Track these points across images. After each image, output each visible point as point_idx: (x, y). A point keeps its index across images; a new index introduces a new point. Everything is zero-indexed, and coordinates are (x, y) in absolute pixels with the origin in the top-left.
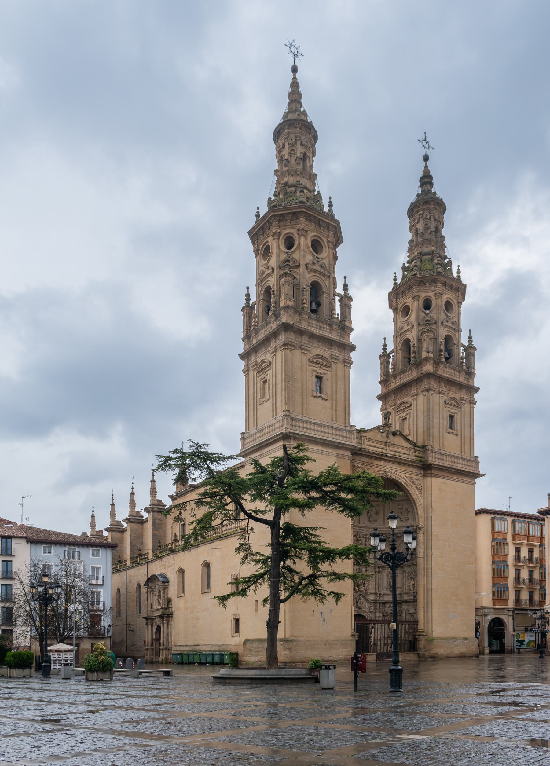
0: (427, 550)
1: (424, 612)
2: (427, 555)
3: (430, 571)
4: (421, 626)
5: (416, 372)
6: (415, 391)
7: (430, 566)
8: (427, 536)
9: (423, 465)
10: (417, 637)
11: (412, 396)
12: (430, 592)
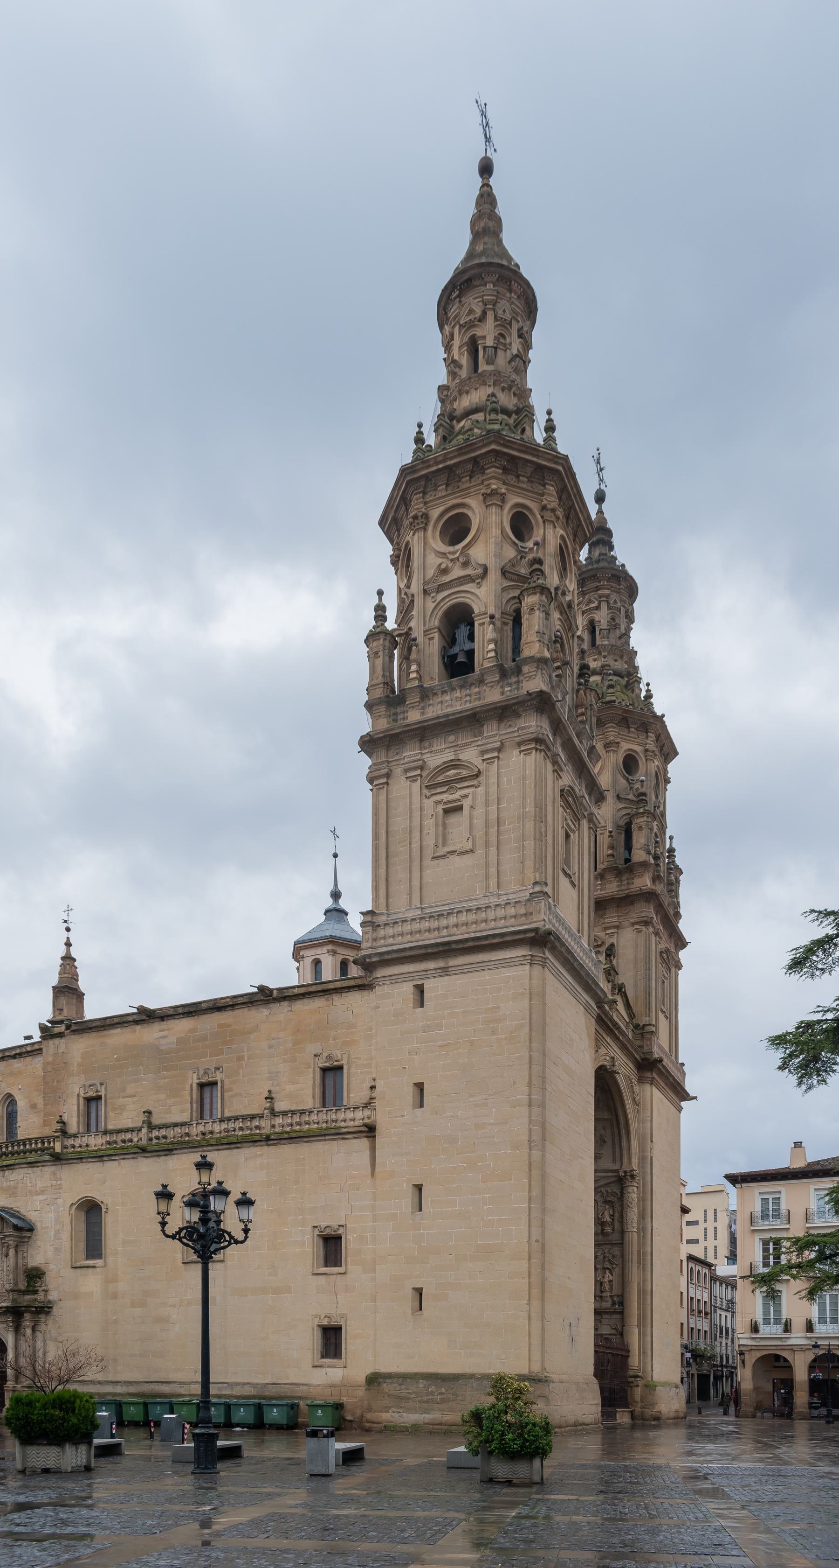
0: (643, 1218)
1: (639, 1334)
2: (644, 1229)
4: (634, 1361)
6: (615, 919)
8: (644, 1192)
9: (643, 1059)
10: (630, 1380)
11: (606, 929)
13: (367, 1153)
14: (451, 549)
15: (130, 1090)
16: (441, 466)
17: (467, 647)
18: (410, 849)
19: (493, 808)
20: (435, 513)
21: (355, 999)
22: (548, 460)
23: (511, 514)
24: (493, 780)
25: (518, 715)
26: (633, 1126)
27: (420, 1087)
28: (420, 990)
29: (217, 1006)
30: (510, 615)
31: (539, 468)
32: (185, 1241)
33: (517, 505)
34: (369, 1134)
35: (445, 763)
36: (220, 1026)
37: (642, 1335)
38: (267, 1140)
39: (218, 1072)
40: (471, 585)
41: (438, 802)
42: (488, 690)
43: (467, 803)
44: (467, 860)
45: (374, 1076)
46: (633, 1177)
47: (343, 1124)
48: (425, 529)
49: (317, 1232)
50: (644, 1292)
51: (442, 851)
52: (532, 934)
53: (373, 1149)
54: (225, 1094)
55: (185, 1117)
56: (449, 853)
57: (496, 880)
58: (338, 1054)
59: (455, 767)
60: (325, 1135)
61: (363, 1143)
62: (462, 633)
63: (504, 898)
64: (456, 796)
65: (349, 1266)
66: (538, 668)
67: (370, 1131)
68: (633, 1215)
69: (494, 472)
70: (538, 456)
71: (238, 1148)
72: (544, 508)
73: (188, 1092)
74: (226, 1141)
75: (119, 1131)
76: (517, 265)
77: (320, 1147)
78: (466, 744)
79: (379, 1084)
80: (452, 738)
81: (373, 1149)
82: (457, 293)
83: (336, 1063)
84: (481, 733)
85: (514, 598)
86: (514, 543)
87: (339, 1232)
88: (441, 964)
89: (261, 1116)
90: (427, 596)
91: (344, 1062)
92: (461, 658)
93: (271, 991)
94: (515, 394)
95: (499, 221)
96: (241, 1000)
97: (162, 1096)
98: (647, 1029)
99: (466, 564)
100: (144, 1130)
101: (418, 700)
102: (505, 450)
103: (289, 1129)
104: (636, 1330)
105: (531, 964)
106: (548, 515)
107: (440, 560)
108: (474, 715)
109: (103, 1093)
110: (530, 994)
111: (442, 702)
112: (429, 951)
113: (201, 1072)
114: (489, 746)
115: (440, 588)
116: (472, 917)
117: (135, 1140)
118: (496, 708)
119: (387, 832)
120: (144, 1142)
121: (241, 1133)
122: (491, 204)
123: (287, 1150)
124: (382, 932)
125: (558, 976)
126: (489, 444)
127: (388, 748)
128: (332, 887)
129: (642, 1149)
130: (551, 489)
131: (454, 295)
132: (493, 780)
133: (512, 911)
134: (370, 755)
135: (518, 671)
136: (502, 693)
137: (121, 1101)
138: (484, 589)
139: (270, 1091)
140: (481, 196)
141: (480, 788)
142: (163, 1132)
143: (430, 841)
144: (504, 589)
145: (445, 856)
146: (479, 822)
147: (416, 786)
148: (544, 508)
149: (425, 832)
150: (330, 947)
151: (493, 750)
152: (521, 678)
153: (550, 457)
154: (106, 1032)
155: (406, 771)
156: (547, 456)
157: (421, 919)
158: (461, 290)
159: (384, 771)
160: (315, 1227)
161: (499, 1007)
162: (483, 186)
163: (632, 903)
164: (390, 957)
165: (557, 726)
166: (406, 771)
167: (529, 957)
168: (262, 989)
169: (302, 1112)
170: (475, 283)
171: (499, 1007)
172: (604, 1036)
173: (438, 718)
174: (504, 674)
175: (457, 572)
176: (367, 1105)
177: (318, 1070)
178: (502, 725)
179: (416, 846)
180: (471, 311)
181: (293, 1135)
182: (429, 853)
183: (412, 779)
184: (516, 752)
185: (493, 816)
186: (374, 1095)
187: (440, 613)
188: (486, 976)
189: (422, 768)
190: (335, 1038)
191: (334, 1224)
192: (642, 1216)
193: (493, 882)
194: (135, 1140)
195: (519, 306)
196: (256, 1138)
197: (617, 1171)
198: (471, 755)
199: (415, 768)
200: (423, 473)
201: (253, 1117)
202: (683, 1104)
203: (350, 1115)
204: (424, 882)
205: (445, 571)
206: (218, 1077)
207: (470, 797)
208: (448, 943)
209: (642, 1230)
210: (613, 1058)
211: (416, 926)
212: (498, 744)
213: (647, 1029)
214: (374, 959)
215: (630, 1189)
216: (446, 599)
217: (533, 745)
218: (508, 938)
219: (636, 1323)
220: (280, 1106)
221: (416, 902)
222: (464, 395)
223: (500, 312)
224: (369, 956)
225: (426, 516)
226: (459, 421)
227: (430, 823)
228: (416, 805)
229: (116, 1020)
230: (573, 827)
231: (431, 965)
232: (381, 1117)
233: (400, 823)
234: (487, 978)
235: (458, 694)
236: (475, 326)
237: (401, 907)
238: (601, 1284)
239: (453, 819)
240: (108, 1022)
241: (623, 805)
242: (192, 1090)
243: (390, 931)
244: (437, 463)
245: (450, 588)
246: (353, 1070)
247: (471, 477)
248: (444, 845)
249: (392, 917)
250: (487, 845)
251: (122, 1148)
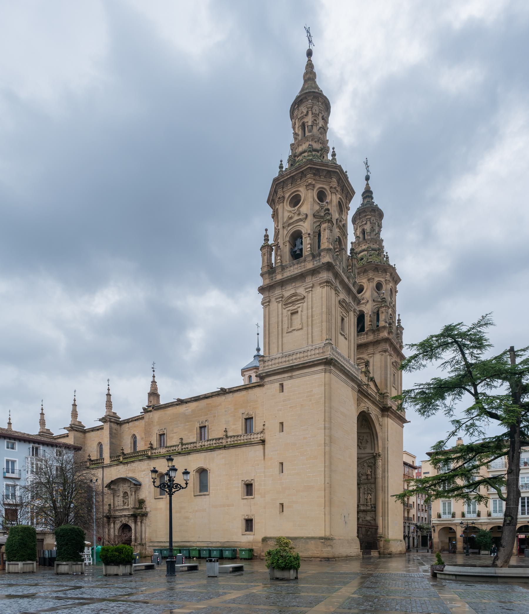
0: (384, 472)
1: (382, 520)
2: (384, 477)
3: (387, 488)
4: (380, 531)
5: (372, 336)
6: (372, 351)
7: (387, 485)
8: (384, 462)
9: (383, 407)
10: (378, 538)
11: (368, 355)
12: (387, 505)
13: (262, 451)
14: (293, 209)
15: (175, 431)
16: (289, 176)
17: (300, 247)
18: (278, 330)
19: (310, 311)
20: (287, 196)
21: (257, 390)
22: (332, 168)
23: (317, 192)
24: (310, 300)
25: (319, 273)
26: (380, 435)
28: (282, 385)
29: (206, 397)
30: (317, 233)
31: (329, 172)
32: (162, 488)
33: (320, 188)
35: (291, 294)
36: (207, 404)
37: (384, 520)
38: (225, 447)
39: (206, 422)
40: (301, 222)
41: (288, 311)
42: (308, 264)
44: (300, 332)
45: (264, 420)
46: (379, 455)
47: (253, 440)
48: (283, 202)
49: (243, 483)
50: (385, 502)
51: (290, 330)
52: (325, 360)
53: (264, 449)
54: (209, 430)
55: (195, 440)
57: (311, 339)
58: (251, 412)
59: (295, 296)
60: (246, 445)
61: (260, 447)
62: (298, 242)
63: (314, 346)
64: (295, 307)
65: (255, 496)
66: (327, 253)
67: (263, 442)
68: (379, 471)
69: (310, 176)
70: (328, 167)
72: (331, 188)
73: (196, 430)
74: (209, 448)
75: (171, 447)
76: (321, 91)
77: (244, 449)
78: (300, 286)
79: (266, 424)
80: (294, 284)
81: (264, 449)
82: (297, 106)
83: (250, 416)
84: (305, 281)
85: (318, 226)
86: (319, 203)
87: (252, 482)
88: (290, 374)
89: (222, 438)
90: (284, 229)
91: (253, 416)
93: (226, 390)
94: (320, 143)
95: (315, 74)
96: (215, 394)
97: (186, 432)
98: (386, 395)
99: (299, 214)
100: (180, 446)
102: (314, 167)
103: (233, 443)
104: (381, 518)
105: (325, 372)
106: (333, 190)
107: (289, 214)
108: (302, 274)
109: (165, 432)
110: (325, 384)
111: (290, 270)
112: (285, 370)
113: (200, 423)
114: (308, 286)
115: (289, 225)
116: (302, 355)
117: (177, 449)
118: (310, 271)
119: (269, 324)
120: (180, 450)
121: (215, 445)
122: (311, 68)
123: (232, 451)
124: (267, 364)
125: (338, 376)
126: (308, 165)
127: (269, 291)
128: (257, 347)
129: (384, 444)
130: (334, 180)
131: (296, 107)
132: (310, 300)
133: (317, 351)
134: (262, 294)
135: (319, 255)
136: (313, 264)
137: (172, 435)
138: (306, 223)
139: (226, 429)
140: (307, 65)
142: (187, 446)
143: (285, 326)
144: (314, 223)
146: (304, 317)
147: (280, 305)
148: (331, 188)
149: (284, 323)
150: (255, 370)
151: (309, 288)
152: (321, 257)
153: (333, 167)
154: (166, 409)
155: (276, 299)
156: (332, 167)
157: (282, 357)
158: (298, 105)
159: (267, 300)
160: (242, 480)
161: (312, 390)
162: (308, 61)
163: (379, 343)
164: (270, 373)
165: (336, 275)
166: (276, 299)
168: (222, 389)
169: (238, 436)
170: (304, 101)
171: (312, 390)
172: (364, 399)
173: (288, 277)
174: (314, 256)
175: (296, 218)
176: (262, 432)
177: (243, 419)
178: (313, 277)
179: (280, 328)
180: (302, 112)
181: (235, 445)
182: (285, 331)
183: (279, 302)
184: (319, 287)
185: (310, 314)
186: (264, 428)
187: (289, 235)
188: (307, 378)
189: (282, 297)
190: (250, 407)
191: (250, 479)
192: (384, 471)
193: (310, 340)
194: (177, 449)
195: (322, 107)
196: (221, 447)
197: (373, 453)
198: (301, 291)
199: (280, 298)
201: (219, 439)
202: (404, 425)
203: (256, 436)
204: (283, 342)
205: (291, 218)
206: (207, 424)
207: (301, 308)
208: (292, 366)
209: (383, 477)
210: (368, 408)
211: (280, 360)
212: (311, 285)
213: (386, 395)
214: (264, 375)
215: (378, 461)
216: (292, 229)
217: (326, 284)
218: (315, 363)
219: (381, 515)
220: (230, 434)
221: (280, 351)
223: (314, 111)
224: (262, 373)
225: (284, 197)
226: (298, 157)
227: (285, 319)
228: (280, 312)
229: (170, 404)
230: (345, 315)
231: (286, 375)
232: (267, 437)
233: (274, 320)
235: (296, 266)
236: (304, 118)
237: (274, 353)
238: (367, 499)
239: (295, 317)
240: (167, 405)
241: (376, 304)
242: (197, 429)
243: (270, 363)
244: (287, 176)
245: (293, 224)
246: (257, 418)
247: (301, 179)
248: (291, 327)
249: (271, 357)
250: (308, 326)
251: (172, 453)
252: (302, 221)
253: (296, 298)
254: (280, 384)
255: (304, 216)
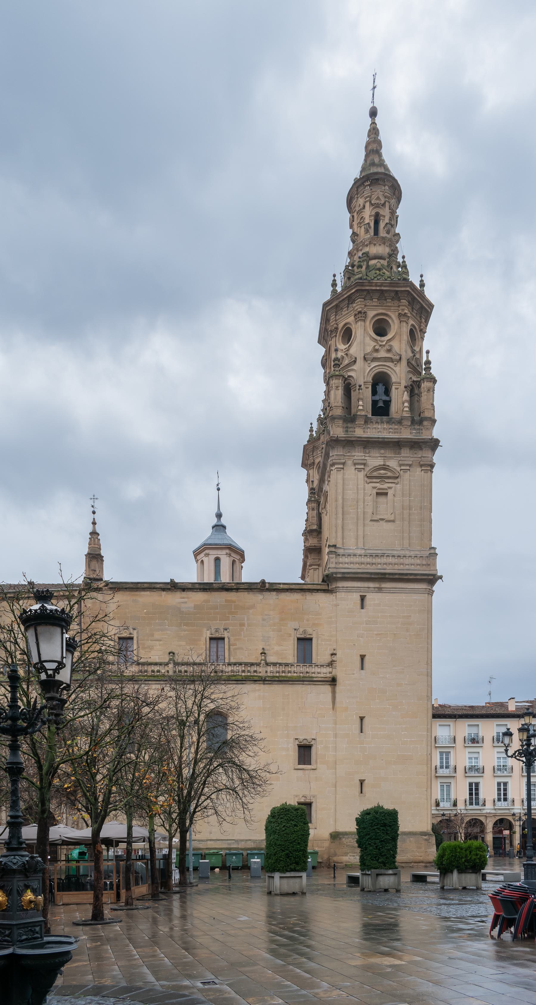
13: (330, 695)
15: (157, 635)
17: (385, 398)
21: (321, 597)
27: (363, 657)
28: (363, 598)
34: (332, 683)
35: (380, 465)
36: (227, 601)
38: (263, 680)
39: (225, 632)
42: (403, 429)
43: (390, 492)
44: (390, 526)
45: (335, 647)
47: (313, 675)
49: (297, 743)
53: (334, 693)
54: (231, 647)
56: (380, 519)
58: (310, 630)
59: (385, 469)
60: (303, 681)
61: (327, 689)
62: (381, 388)
64: (386, 486)
67: (333, 681)
71: (243, 684)
74: (234, 678)
77: (299, 688)
78: (390, 457)
79: (339, 653)
80: (382, 451)
81: (334, 693)
83: (308, 636)
84: (399, 453)
87: (312, 743)
88: (377, 585)
89: (258, 664)
91: (314, 636)
92: (381, 404)
97: (183, 643)
100: (171, 666)
101: (363, 423)
103: (278, 674)
108: (398, 442)
109: (135, 635)
110: (428, 611)
111: (375, 428)
112: (373, 576)
113: (213, 631)
114: (406, 462)
115: (375, 359)
120: (171, 673)
121: (243, 674)
123: (277, 688)
133: (418, 561)
137: (150, 643)
139: (263, 649)
141: (398, 485)
143: (369, 510)
145: (378, 520)
147: (361, 475)
149: (366, 503)
151: (407, 465)
155: (355, 464)
159: (343, 461)
160: (296, 739)
161: (410, 616)
164: (348, 576)
167: (428, 590)
168: (263, 582)
169: (287, 665)
171: (410, 616)
173: (379, 438)
176: (331, 664)
177: (296, 639)
181: (281, 679)
182: (369, 516)
183: (359, 470)
184: (419, 469)
186: (334, 659)
187: (373, 374)
188: (403, 596)
189: (364, 464)
190: (308, 620)
191: (309, 738)
193: (406, 542)
196: (256, 678)
199: (361, 464)
200: (367, 288)
201: (252, 664)
203: (317, 670)
206: (226, 635)
207: (393, 489)
214: (339, 576)
220: (271, 659)
221: (361, 545)
222: (372, 245)
224: (336, 573)
229: (146, 586)
231: (371, 585)
232: (339, 672)
234: (404, 598)
240: (139, 585)
243: (347, 560)
246: (320, 642)
251: (151, 676)
252: (393, 362)
253: (386, 473)
254: (361, 596)
255: (398, 357)
